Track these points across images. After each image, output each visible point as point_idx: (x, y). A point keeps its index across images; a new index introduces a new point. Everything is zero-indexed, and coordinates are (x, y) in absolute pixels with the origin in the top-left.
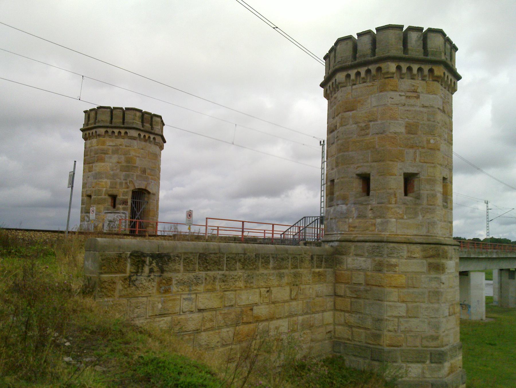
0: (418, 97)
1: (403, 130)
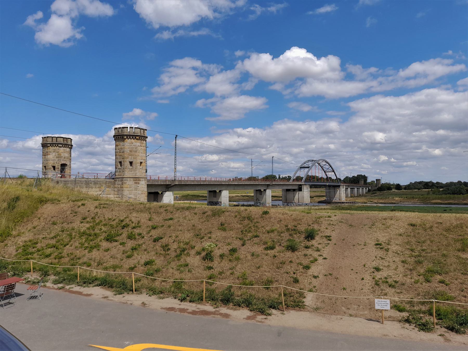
0: (132, 144)
1: (129, 151)
